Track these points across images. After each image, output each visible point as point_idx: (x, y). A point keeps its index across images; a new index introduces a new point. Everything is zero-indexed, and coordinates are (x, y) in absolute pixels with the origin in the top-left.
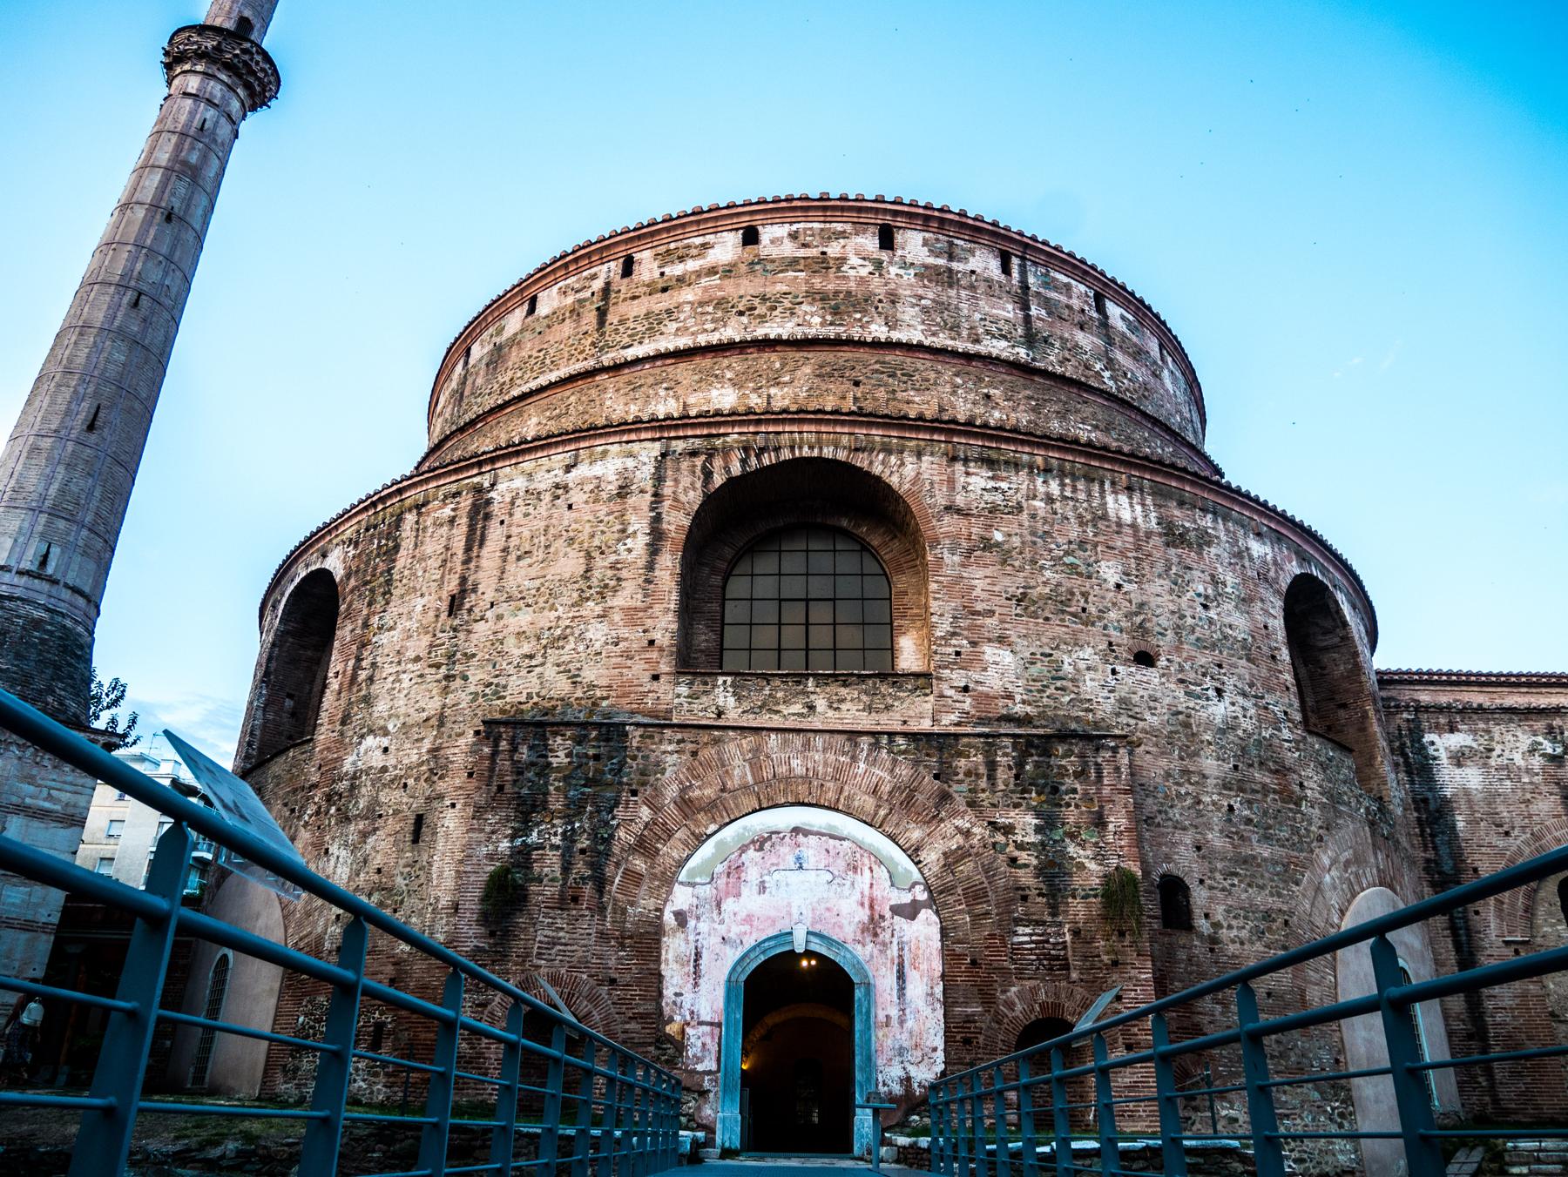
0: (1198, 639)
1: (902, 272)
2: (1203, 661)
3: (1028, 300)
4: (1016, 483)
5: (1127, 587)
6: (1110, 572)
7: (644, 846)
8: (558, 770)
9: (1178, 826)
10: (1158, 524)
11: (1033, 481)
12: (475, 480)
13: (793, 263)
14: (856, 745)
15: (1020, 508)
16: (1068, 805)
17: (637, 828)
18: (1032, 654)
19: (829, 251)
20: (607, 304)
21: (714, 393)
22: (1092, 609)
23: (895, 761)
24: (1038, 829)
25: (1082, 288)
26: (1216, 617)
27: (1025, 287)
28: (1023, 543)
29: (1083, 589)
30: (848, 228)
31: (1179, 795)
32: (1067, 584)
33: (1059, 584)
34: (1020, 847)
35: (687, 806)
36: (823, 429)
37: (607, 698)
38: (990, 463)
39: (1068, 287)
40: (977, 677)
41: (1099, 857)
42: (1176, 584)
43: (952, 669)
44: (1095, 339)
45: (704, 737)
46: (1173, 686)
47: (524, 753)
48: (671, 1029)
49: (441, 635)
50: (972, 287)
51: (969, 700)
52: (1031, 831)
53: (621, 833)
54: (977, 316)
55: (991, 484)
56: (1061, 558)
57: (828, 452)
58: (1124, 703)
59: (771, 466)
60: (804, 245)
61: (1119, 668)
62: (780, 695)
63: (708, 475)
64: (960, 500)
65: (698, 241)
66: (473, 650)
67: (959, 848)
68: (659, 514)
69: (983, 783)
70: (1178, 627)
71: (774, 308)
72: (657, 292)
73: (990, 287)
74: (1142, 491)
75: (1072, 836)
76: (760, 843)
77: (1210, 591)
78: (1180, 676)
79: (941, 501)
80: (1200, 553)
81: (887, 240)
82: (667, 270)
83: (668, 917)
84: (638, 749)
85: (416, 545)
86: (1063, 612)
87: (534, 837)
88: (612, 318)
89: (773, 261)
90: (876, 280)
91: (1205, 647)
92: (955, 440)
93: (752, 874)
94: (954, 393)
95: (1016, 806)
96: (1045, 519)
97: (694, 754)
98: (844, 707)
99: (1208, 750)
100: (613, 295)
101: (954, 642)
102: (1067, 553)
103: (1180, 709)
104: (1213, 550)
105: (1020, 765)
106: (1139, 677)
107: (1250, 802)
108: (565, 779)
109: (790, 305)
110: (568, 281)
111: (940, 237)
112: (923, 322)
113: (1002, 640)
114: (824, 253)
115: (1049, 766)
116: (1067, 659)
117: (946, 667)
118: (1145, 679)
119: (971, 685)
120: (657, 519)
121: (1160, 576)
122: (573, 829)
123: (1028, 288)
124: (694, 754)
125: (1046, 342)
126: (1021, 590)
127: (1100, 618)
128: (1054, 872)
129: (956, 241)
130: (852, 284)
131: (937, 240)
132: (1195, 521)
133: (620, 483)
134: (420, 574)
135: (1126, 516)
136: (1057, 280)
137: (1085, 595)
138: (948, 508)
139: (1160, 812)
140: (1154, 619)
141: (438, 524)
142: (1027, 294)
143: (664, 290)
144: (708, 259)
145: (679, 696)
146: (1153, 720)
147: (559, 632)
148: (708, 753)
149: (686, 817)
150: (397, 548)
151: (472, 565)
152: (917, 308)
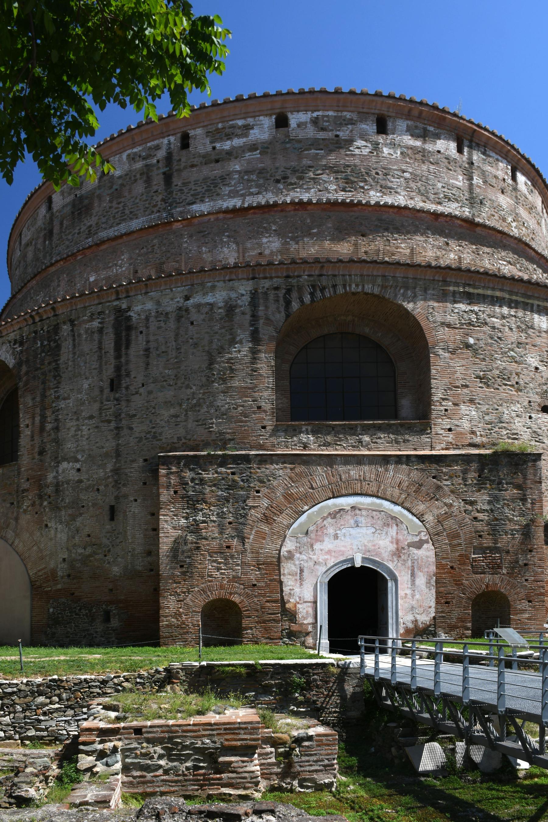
12: (115, 303)
20: (170, 169)
21: (265, 240)
40: (456, 422)
49: (107, 403)
51: (451, 436)
66: (134, 412)
72: (211, 162)
82: (218, 145)
85: (74, 345)
88: (177, 181)
100: (175, 163)
110: (135, 150)
127: (525, 387)
134: (82, 364)
143: (217, 161)
144: (250, 138)
150: (58, 347)
151: (123, 360)
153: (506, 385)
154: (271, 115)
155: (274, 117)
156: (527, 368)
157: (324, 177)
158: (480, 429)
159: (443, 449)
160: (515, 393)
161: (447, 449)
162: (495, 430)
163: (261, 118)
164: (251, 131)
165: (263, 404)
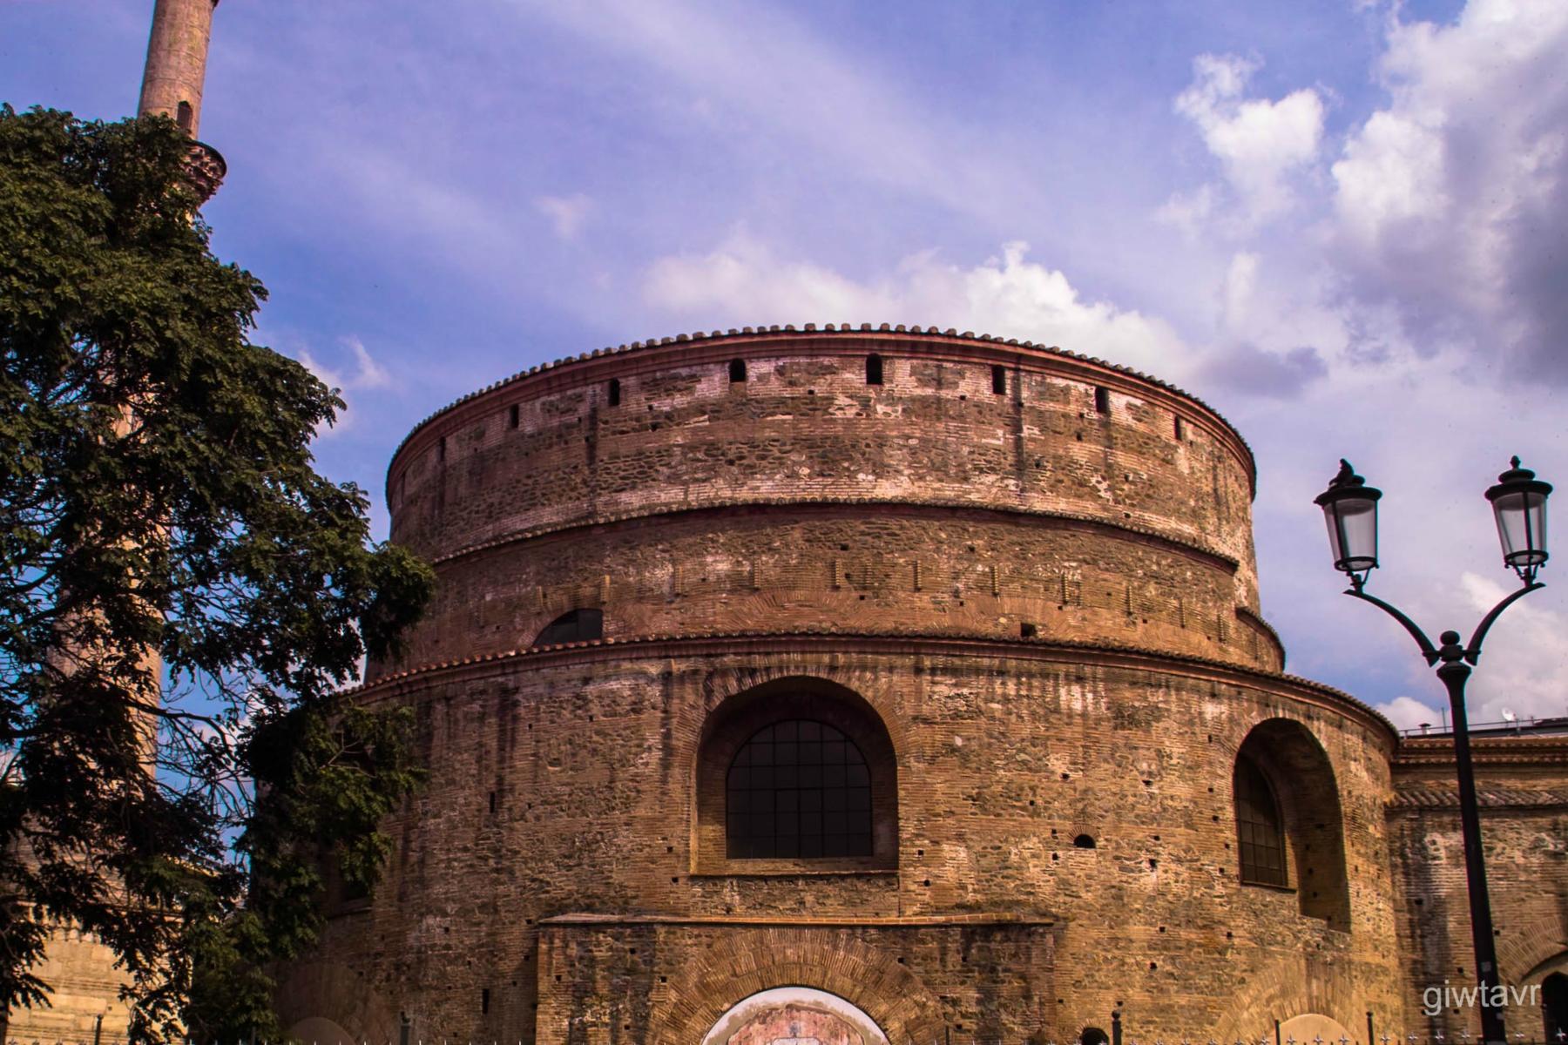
0: (1137, 816)
2: (1140, 835)
3: (1021, 419)
4: (975, 687)
6: (1058, 764)
7: (675, 1023)
8: (603, 962)
9: (1104, 987)
10: (1108, 709)
11: (992, 683)
14: (838, 935)
15: (980, 712)
16: (1003, 982)
18: (985, 848)
19: (816, 389)
23: (868, 949)
24: (979, 1002)
25: (1082, 387)
26: (1156, 791)
27: (1018, 404)
28: (980, 745)
29: (1032, 783)
31: (1106, 959)
32: (1018, 780)
33: (1011, 782)
34: (964, 1016)
35: (705, 988)
37: (635, 897)
39: (1066, 391)
40: (936, 872)
41: (1025, 1023)
42: (1119, 766)
43: (915, 867)
44: (1093, 447)
45: (718, 932)
46: (1108, 864)
47: (574, 950)
50: (961, 417)
51: (928, 893)
53: (656, 1011)
55: (955, 691)
56: (1013, 757)
58: (1064, 885)
59: (764, 685)
61: (1060, 853)
63: (709, 693)
64: (925, 709)
67: (917, 1018)
68: (669, 730)
69: (937, 965)
70: (1119, 807)
73: (980, 413)
75: (1005, 1006)
78: (1116, 853)
79: (910, 712)
80: (1147, 731)
81: (875, 376)
84: (665, 943)
87: (588, 1018)
91: (1143, 823)
95: (963, 983)
98: (828, 902)
99: (1136, 918)
101: (918, 843)
103: (1114, 883)
105: (967, 949)
106: (1078, 859)
107: (1173, 958)
108: (609, 969)
109: (778, 454)
111: (930, 362)
112: (910, 467)
113: (960, 838)
115: (989, 950)
116: (1014, 850)
117: (911, 865)
118: (1083, 860)
119: (931, 880)
120: (667, 736)
121: (1106, 761)
122: (618, 1010)
123: (1021, 405)
124: (709, 946)
125: (1038, 466)
126: (976, 790)
127: (1046, 809)
129: (946, 365)
131: (926, 366)
132: (1146, 699)
133: (633, 698)
135: (1077, 706)
136: (1053, 385)
137: (1033, 789)
138: (915, 718)
140: (1097, 803)
141: (468, 718)
142: (1018, 412)
145: (694, 896)
147: (590, 837)
149: (705, 997)
152: (905, 451)
154: (723, 362)
155: (727, 365)
157: (794, 457)
158: (973, 881)
159: (916, 915)
160: (1029, 819)
161: (921, 913)
163: (711, 366)
164: (698, 386)
165: (674, 844)
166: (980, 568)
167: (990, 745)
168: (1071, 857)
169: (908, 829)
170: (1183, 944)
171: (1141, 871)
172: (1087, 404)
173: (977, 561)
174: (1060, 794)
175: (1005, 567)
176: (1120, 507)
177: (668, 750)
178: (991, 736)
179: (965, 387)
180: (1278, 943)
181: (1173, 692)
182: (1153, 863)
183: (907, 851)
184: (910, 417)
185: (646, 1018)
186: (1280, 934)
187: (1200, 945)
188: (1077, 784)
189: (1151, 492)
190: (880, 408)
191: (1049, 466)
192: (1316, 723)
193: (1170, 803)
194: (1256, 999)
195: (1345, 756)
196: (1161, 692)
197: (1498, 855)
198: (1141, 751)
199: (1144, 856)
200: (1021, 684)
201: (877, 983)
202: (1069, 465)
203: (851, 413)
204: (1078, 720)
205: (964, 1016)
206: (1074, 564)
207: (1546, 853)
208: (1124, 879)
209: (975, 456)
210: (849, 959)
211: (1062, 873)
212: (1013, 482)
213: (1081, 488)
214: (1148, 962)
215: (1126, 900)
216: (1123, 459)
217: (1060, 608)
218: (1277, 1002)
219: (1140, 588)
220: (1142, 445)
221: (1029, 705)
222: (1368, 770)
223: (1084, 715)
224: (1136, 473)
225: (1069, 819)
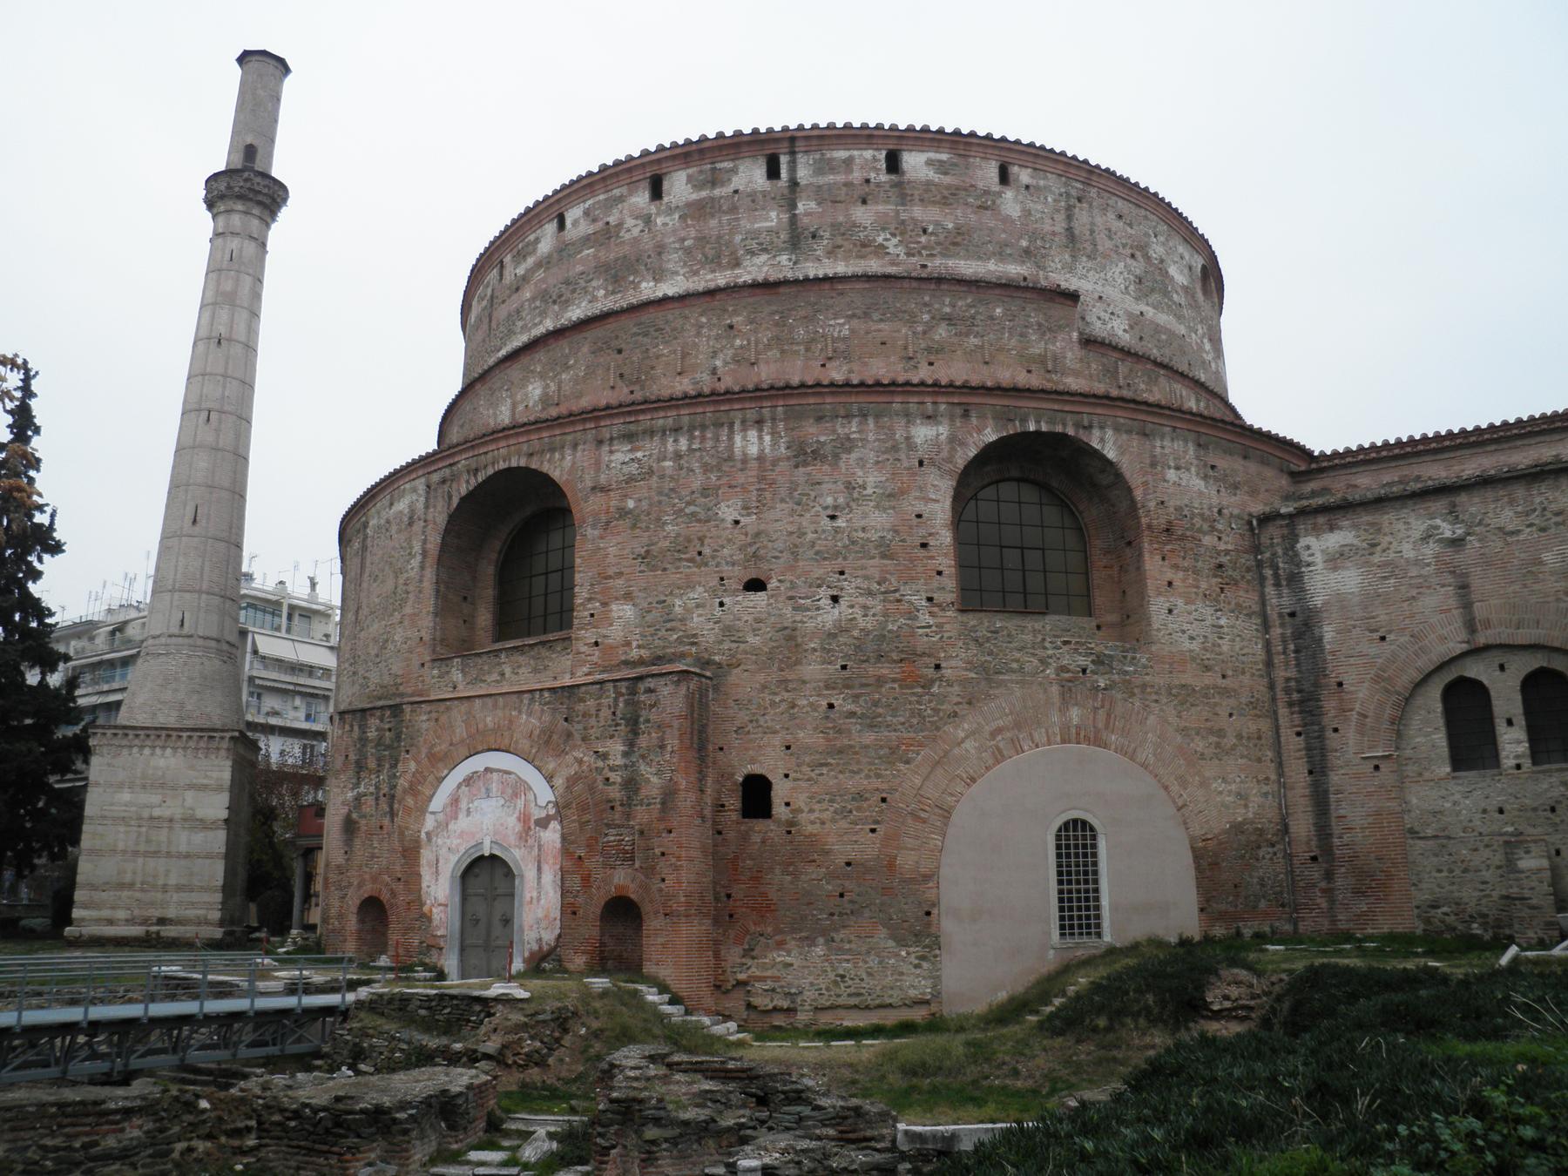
0: (817, 553)
1: (667, 220)
2: (819, 572)
4: (647, 450)
5: (743, 520)
7: (413, 790)
8: (371, 741)
10: (788, 448)
11: (663, 442)
13: (587, 240)
15: (651, 472)
17: (409, 776)
18: (650, 603)
22: (707, 551)
25: (868, 154)
27: (794, 184)
29: (700, 534)
30: (624, 190)
31: (773, 704)
33: (678, 535)
34: (612, 769)
36: (512, 441)
38: (629, 437)
39: (848, 162)
40: (604, 632)
41: (659, 773)
42: (799, 504)
44: (881, 208)
45: (442, 706)
48: (426, 909)
51: (597, 653)
52: (619, 757)
54: (738, 238)
56: (681, 510)
57: (514, 464)
58: (728, 631)
60: (594, 220)
61: (726, 600)
62: (486, 668)
63: (450, 497)
64: (603, 479)
65: (532, 237)
70: (796, 546)
71: (574, 291)
73: (753, 201)
74: (773, 419)
75: (643, 757)
76: (468, 781)
77: (841, 500)
78: (790, 594)
79: (589, 484)
83: (423, 836)
86: (680, 560)
87: (362, 789)
89: (573, 244)
90: (646, 235)
91: (825, 559)
92: (602, 424)
93: (463, 805)
94: (698, 334)
95: (612, 737)
96: (671, 477)
97: (437, 720)
98: (521, 671)
102: (688, 504)
104: (854, 456)
106: (745, 604)
107: (856, 697)
113: (628, 597)
114: (608, 223)
116: (678, 602)
117: (582, 629)
118: (751, 604)
121: (782, 500)
127: (713, 557)
128: (632, 785)
130: (627, 248)
132: (834, 431)
135: (753, 450)
136: (833, 159)
138: (593, 488)
139: (751, 721)
140: (770, 544)
146: (753, 640)
148: (444, 719)
153: (680, 560)
156: (717, 526)
160: (695, 569)
162: (660, 634)
166: (738, 342)
167: (660, 502)
168: (737, 603)
169: (581, 593)
170: (871, 681)
171: (818, 609)
172: (877, 170)
173: (735, 337)
174: (729, 541)
175: (765, 336)
176: (914, 260)
177: (424, 553)
178: (660, 493)
179: (738, 182)
180: (1013, 671)
181: (871, 421)
182: (835, 599)
183: (581, 615)
184: (685, 221)
185: (395, 786)
186: (1017, 661)
187: (894, 680)
188: (749, 529)
189: (959, 239)
190: (659, 221)
191: (827, 235)
192: (1096, 433)
193: (861, 535)
194: (973, 733)
195: (1153, 465)
196: (855, 422)
197: (1384, 551)
198: (824, 486)
199: (824, 593)
200: (694, 438)
201: (547, 742)
202: (845, 231)
203: (636, 232)
204: (754, 464)
205: (612, 769)
206: (842, 321)
207: (1440, 541)
208: (798, 618)
209: (747, 242)
210: (530, 720)
211: (728, 620)
212: (785, 257)
213: (866, 247)
214: (824, 703)
215: (799, 640)
216: (917, 212)
217: (823, 365)
218: (1008, 735)
219: (925, 333)
220: (948, 197)
221: (701, 457)
222: (1205, 478)
223: (761, 458)
224: (937, 224)
225: (739, 565)
